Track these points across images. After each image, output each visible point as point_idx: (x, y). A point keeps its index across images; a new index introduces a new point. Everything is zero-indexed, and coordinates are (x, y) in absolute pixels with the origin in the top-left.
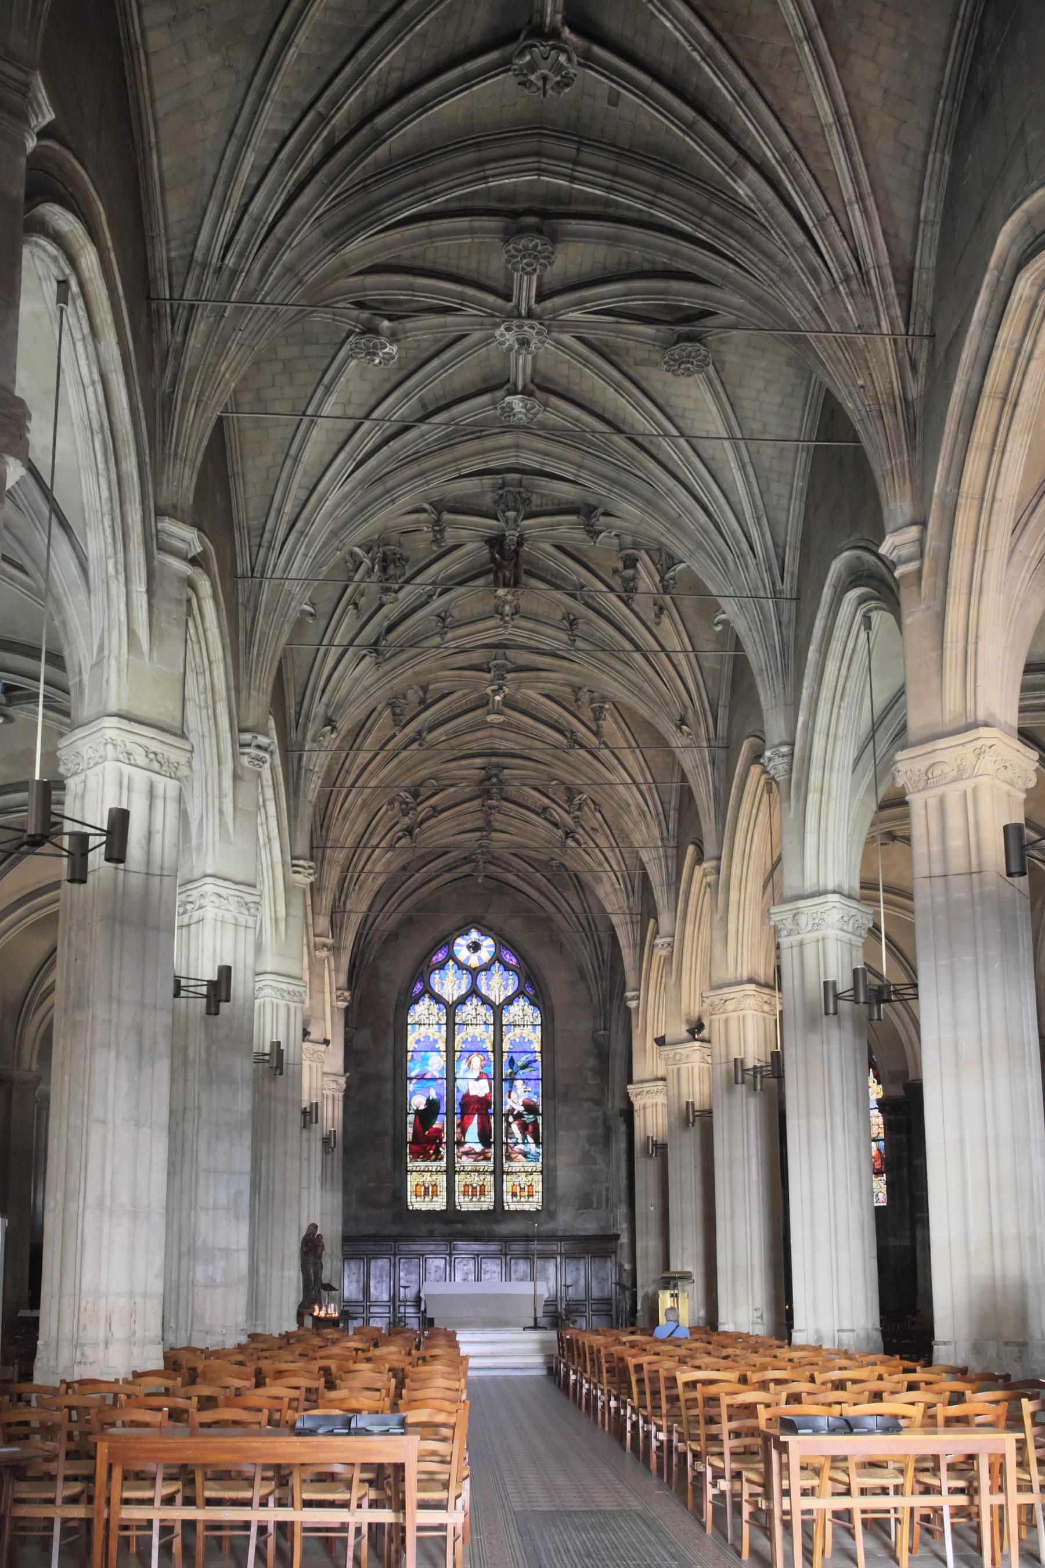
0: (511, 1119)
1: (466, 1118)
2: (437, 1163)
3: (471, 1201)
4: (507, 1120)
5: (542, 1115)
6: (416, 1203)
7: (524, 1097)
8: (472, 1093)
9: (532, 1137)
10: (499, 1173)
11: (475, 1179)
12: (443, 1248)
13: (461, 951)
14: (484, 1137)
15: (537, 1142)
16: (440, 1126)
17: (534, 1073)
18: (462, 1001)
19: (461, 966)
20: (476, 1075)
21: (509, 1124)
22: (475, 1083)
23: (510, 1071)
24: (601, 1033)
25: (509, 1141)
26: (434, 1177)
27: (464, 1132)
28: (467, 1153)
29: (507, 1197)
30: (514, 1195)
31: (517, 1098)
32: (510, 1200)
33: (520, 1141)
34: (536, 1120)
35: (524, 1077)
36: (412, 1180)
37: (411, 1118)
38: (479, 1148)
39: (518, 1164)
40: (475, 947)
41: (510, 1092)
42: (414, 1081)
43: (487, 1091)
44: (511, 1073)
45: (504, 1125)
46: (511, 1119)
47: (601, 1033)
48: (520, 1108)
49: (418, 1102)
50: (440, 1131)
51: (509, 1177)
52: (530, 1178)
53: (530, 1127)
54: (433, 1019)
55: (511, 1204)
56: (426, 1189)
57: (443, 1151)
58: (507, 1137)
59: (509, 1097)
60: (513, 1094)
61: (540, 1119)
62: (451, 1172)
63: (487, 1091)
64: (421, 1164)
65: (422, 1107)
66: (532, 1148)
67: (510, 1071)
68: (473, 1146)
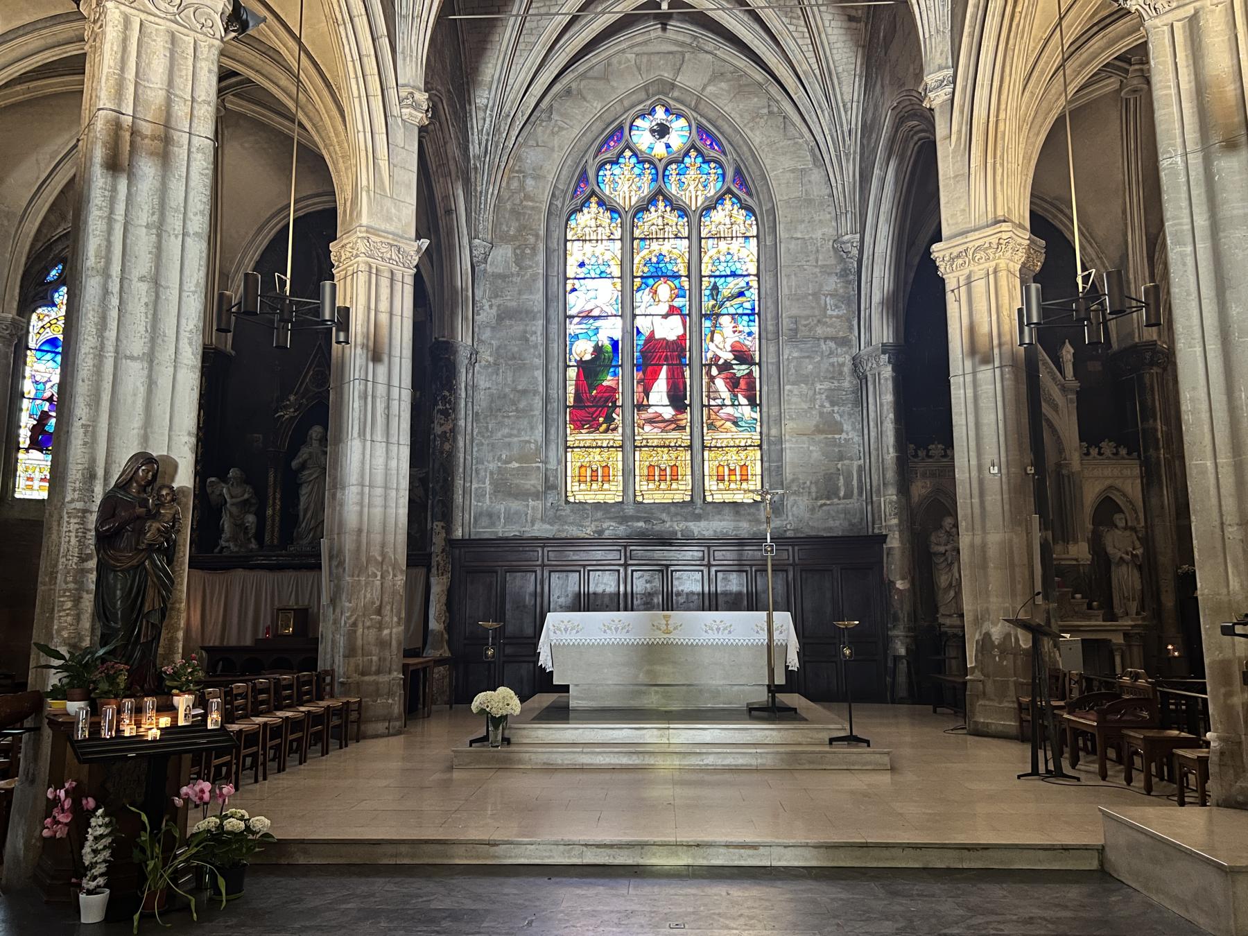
0: (714, 371)
2: (609, 435)
3: (658, 488)
4: (709, 373)
5: (759, 364)
6: (580, 493)
7: (732, 338)
8: (657, 336)
9: (745, 397)
10: (698, 448)
11: (664, 458)
12: (615, 555)
13: (642, 138)
14: (677, 398)
15: (752, 403)
18: (643, 208)
19: (643, 160)
20: (664, 308)
21: (712, 378)
23: (712, 302)
24: (846, 238)
25: (712, 402)
26: (605, 455)
27: (647, 393)
28: (650, 421)
29: (710, 484)
30: (720, 479)
31: (721, 344)
32: (714, 488)
33: (728, 402)
35: (732, 311)
36: (574, 460)
37: (572, 373)
38: (668, 413)
39: (726, 435)
40: (662, 131)
41: (713, 333)
42: (576, 320)
44: (714, 306)
45: (705, 379)
47: (846, 238)
48: (727, 356)
49: (583, 349)
50: (613, 390)
51: (712, 454)
52: (743, 454)
53: (742, 382)
54: (603, 233)
55: (716, 492)
56: (595, 471)
57: (618, 418)
58: (708, 396)
59: (712, 340)
60: (717, 337)
61: (756, 369)
62: (630, 446)
63: (681, 332)
64: (585, 437)
65: (588, 357)
66: (746, 412)
67: (712, 302)
68: (660, 410)
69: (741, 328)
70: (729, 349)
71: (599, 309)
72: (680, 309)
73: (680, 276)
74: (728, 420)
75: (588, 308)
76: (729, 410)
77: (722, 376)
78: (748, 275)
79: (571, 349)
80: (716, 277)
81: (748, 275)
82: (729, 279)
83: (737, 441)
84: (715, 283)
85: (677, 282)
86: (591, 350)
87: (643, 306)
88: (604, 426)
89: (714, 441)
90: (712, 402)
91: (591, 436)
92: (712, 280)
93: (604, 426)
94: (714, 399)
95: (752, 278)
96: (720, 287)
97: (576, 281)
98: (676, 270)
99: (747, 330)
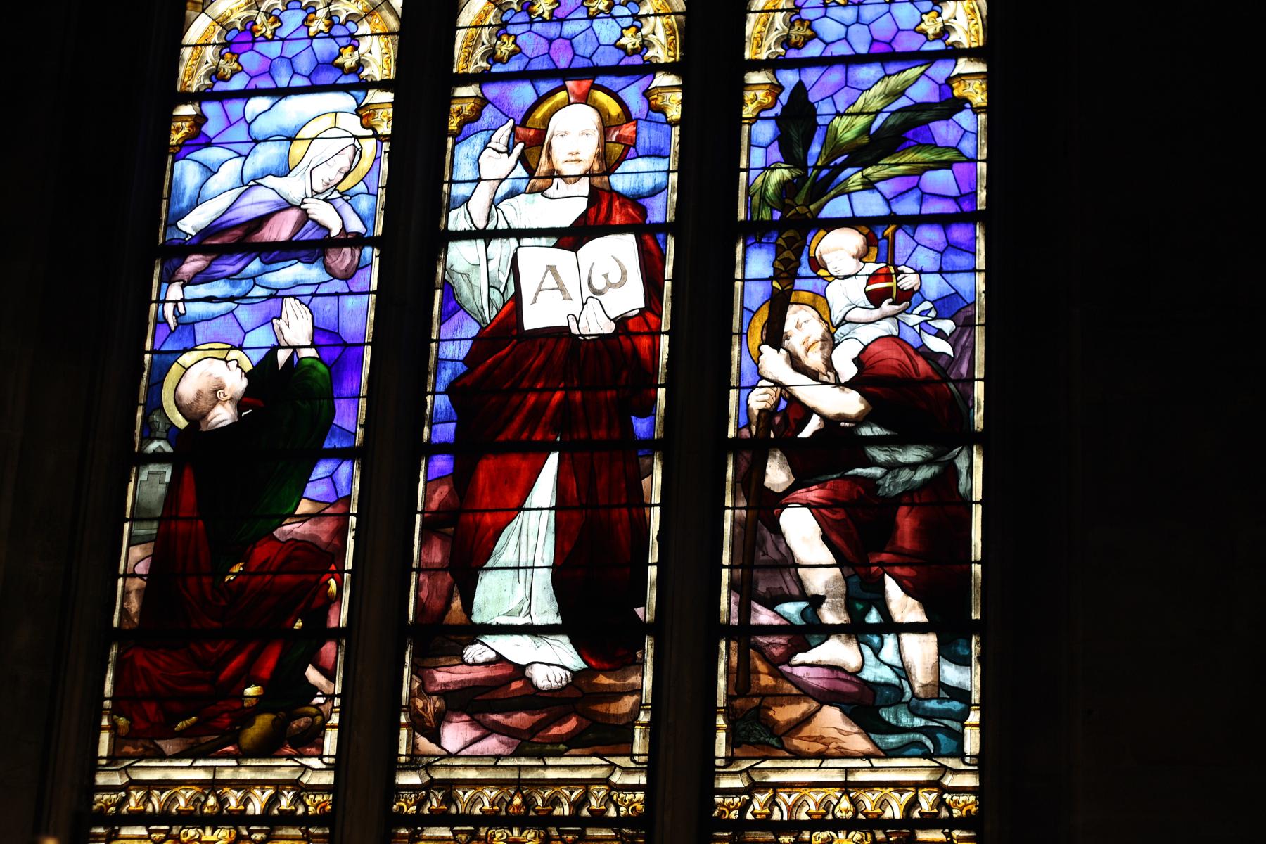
0: (777, 475)
1: (487, 468)
8: (533, 319)
16: (323, 530)
17: (941, 180)
21: (775, 502)
22: (563, 257)
34: (950, 473)
35: (871, 205)
41: (779, 305)
43: (631, 298)
46: (777, 475)
53: (906, 522)
58: (746, 592)
59: (775, 336)
68: (517, 649)
69: (909, 281)
70: (848, 371)
71: (293, 216)
72: (635, 201)
73: (652, 68)
74: (826, 697)
75: (251, 207)
76: (838, 651)
77: (814, 494)
78: (954, 53)
79: (156, 385)
80: (801, 64)
81: (954, 53)
82: (866, 73)
83: (869, 801)
84: (800, 88)
85: (632, 95)
86: (236, 383)
87: (479, 206)
88: (263, 722)
89: (761, 798)
90: (764, 617)
91: (195, 772)
92: (789, 78)
93: (263, 722)
94: (771, 603)
95: (964, 66)
96: (825, 108)
97: (211, 109)
98: (630, 41)
99: (934, 286)
